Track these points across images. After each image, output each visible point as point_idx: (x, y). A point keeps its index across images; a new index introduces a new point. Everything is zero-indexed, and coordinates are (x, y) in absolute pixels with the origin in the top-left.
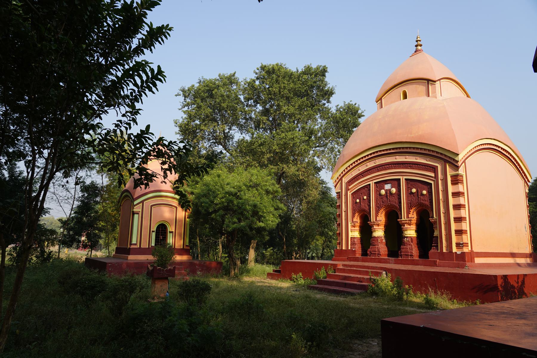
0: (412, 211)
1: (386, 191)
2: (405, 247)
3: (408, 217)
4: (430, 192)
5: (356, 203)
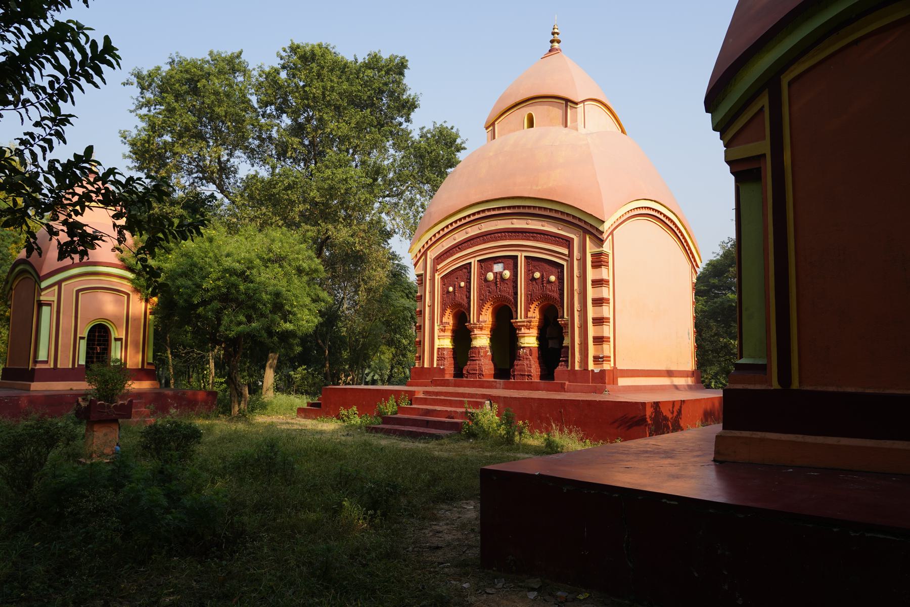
0: (533, 307)
1: (496, 274)
2: (520, 362)
3: (526, 317)
4: (560, 279)
5: (448, 292)
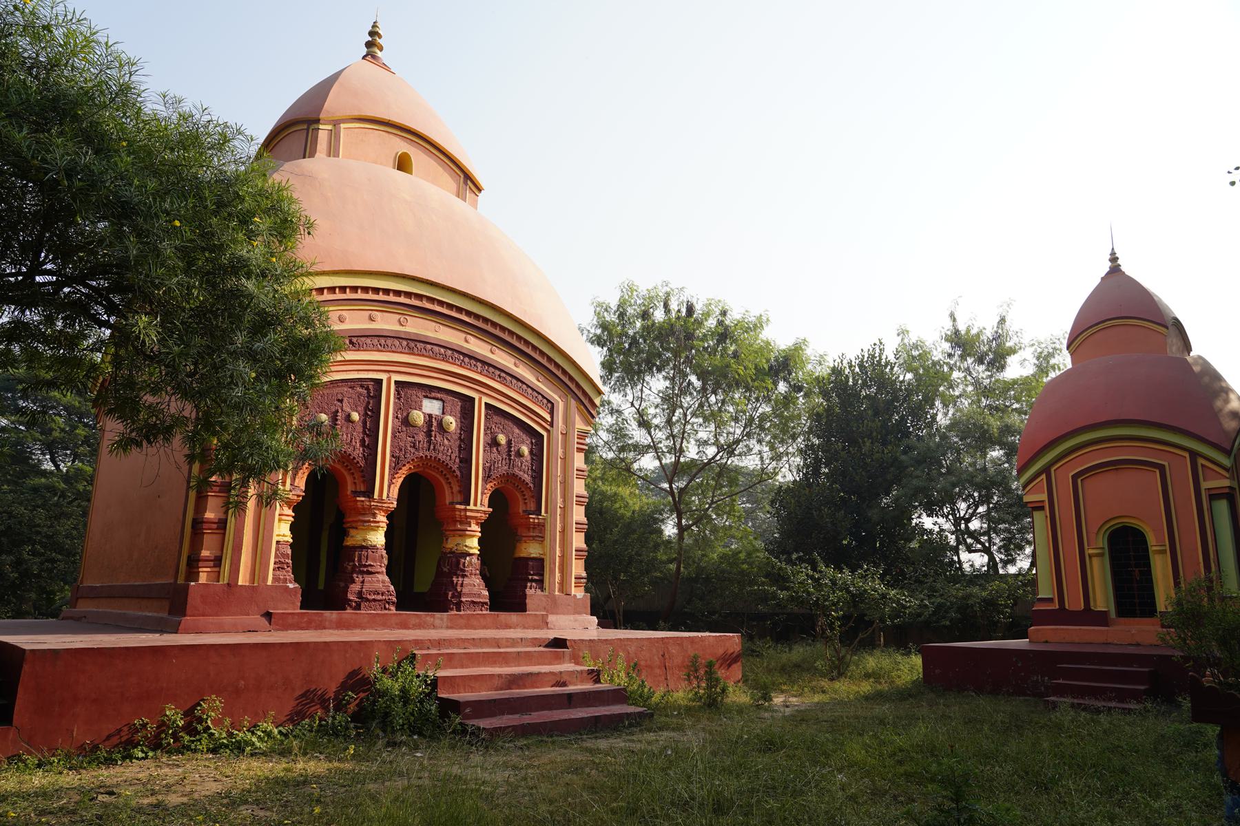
2: (466, 581)
4: (537, 454)
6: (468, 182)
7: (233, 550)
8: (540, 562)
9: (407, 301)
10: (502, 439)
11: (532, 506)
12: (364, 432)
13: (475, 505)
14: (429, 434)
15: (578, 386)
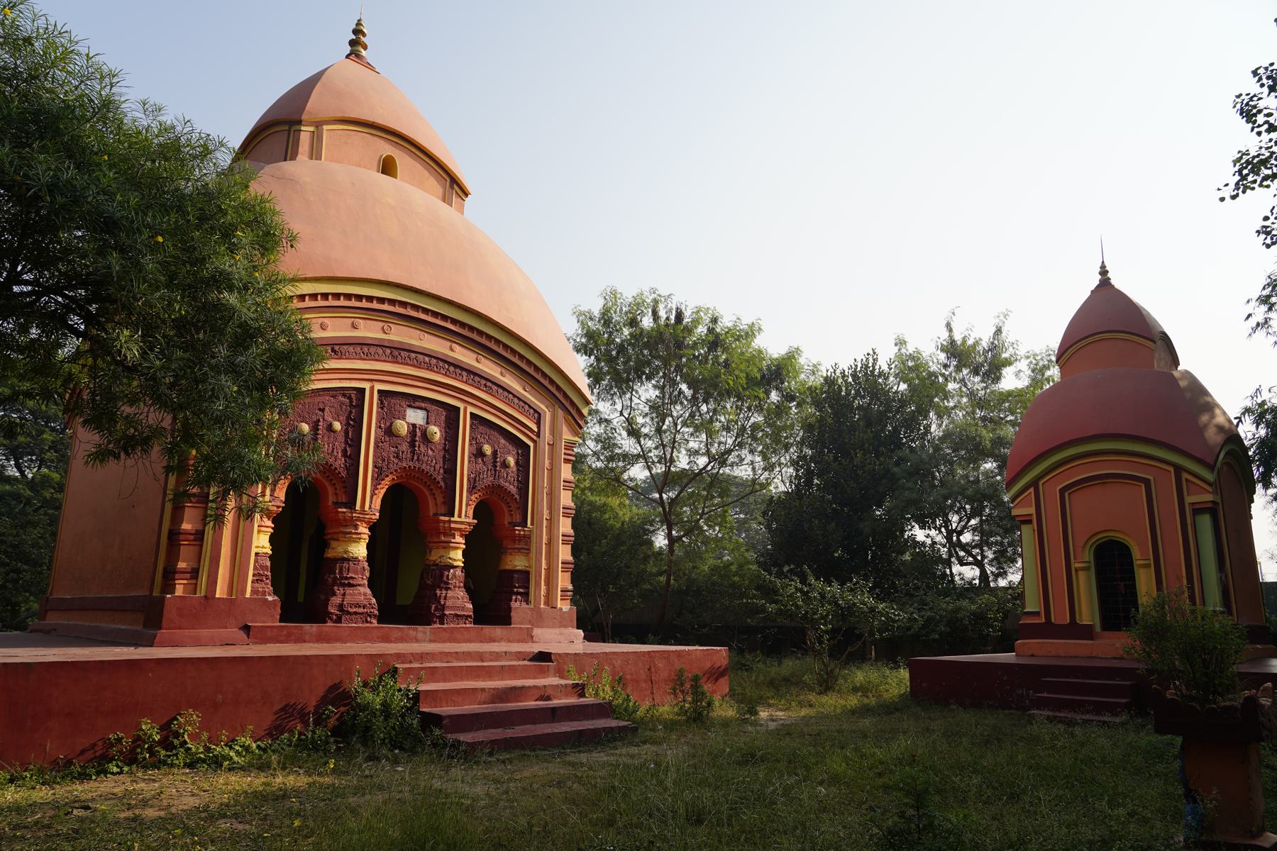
2: (450, 593)
4: (523, 465)
6: (454, 186)
7: (211, 561)
8: (525, 575)
9: (391, 308)
10: (487, 449)
11: (518, 518)
12: (346, 442)
13: (460, 516)
14: (412, 444)
15: (565, 395)
